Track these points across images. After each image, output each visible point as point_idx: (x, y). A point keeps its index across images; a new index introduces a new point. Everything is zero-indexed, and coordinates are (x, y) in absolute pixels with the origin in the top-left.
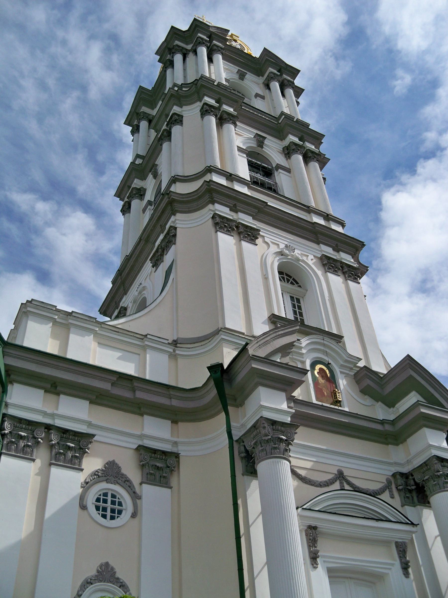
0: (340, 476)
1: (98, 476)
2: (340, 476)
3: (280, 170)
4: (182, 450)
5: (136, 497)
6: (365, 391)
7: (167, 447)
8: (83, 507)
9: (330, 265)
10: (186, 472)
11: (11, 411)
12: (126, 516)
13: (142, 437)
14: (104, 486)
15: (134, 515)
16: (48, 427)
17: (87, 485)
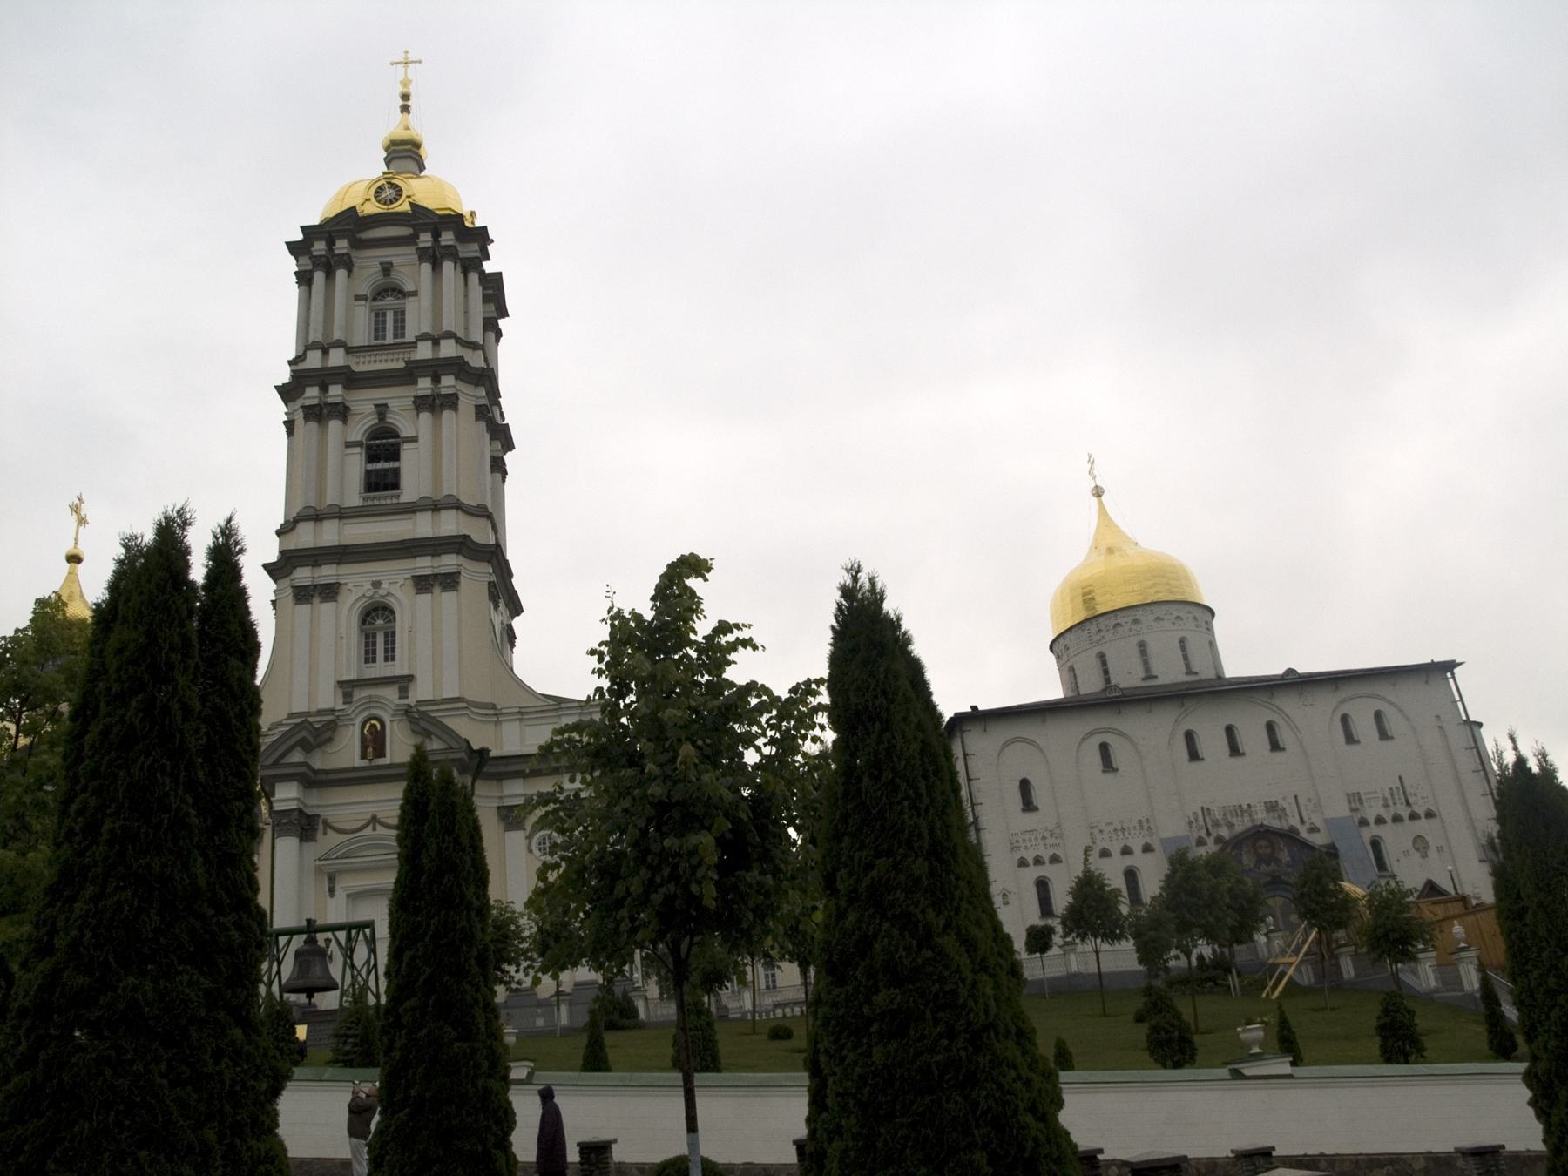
0: (374, 820)
2: (374, 820)
3: (406, 446)
9: (423, 584)
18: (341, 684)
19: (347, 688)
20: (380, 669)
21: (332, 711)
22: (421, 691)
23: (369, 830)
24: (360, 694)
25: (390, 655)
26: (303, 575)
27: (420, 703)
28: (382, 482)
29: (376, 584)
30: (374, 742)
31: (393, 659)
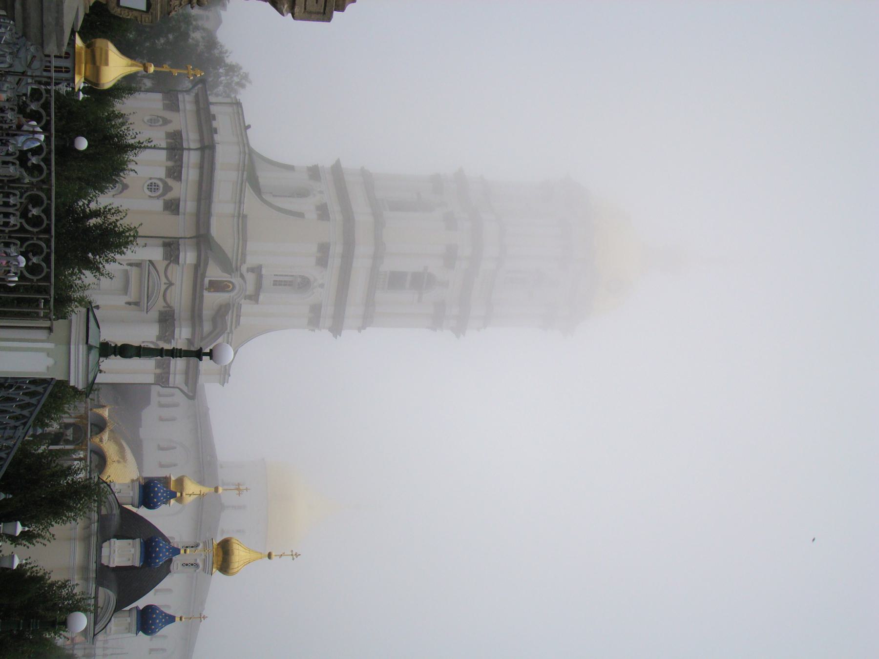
0: (171, 284)
1: (165, 184)
2: (171, 284)
4: (181, 216)
5: (158, 197)
6: (220, 307)
7: (181, 210)
8: (151, 179)
10: (170, 218)
11: (185, 153)
12: (149, 193)
13: (186, 201)
14: (161, 185)
15: (150, 197)
16: (182, 167)
17: (160, 179)
18: (260, 267)
19: (257, 270)
20: (267, 283)
21: (244, 261)
22: (247, 307)
23: (164, 280)
24: (251, 278)
25: (276, 283)
26: (337, 250)
27: (240, 306)
28: (396, 281)
29: (322, 286)
30: (216, 286)
31: (274, 285)
